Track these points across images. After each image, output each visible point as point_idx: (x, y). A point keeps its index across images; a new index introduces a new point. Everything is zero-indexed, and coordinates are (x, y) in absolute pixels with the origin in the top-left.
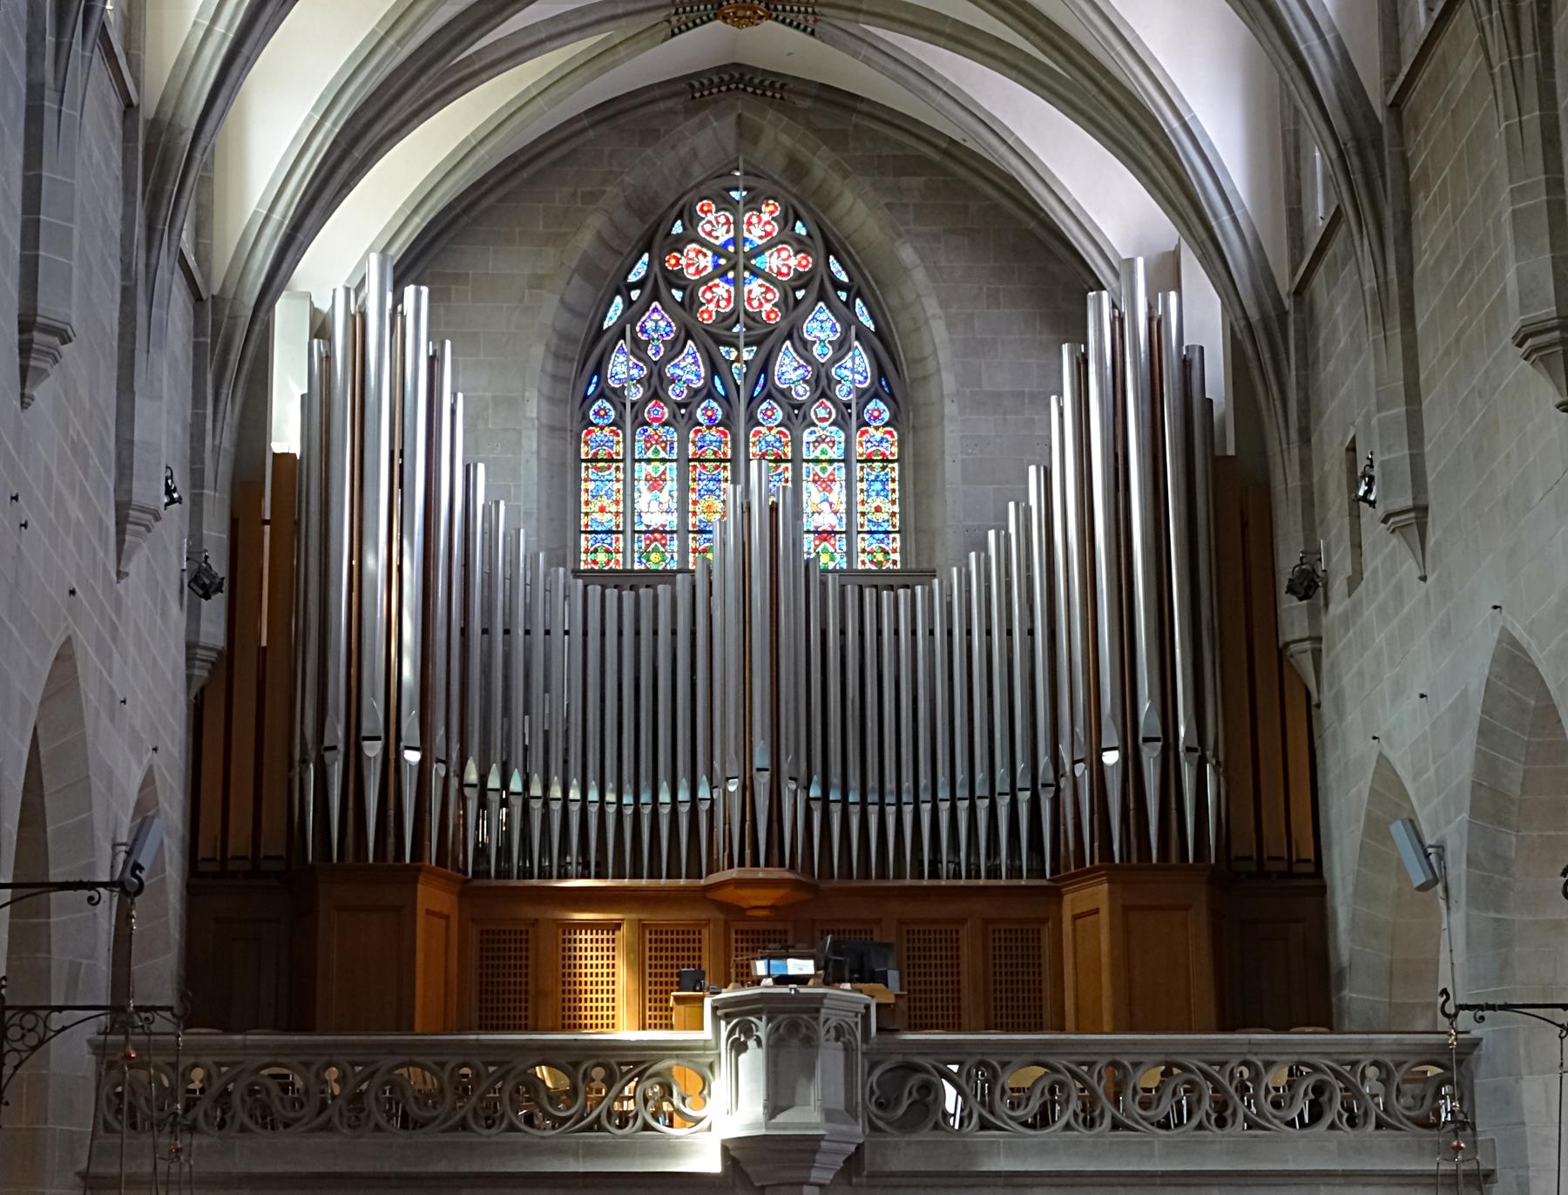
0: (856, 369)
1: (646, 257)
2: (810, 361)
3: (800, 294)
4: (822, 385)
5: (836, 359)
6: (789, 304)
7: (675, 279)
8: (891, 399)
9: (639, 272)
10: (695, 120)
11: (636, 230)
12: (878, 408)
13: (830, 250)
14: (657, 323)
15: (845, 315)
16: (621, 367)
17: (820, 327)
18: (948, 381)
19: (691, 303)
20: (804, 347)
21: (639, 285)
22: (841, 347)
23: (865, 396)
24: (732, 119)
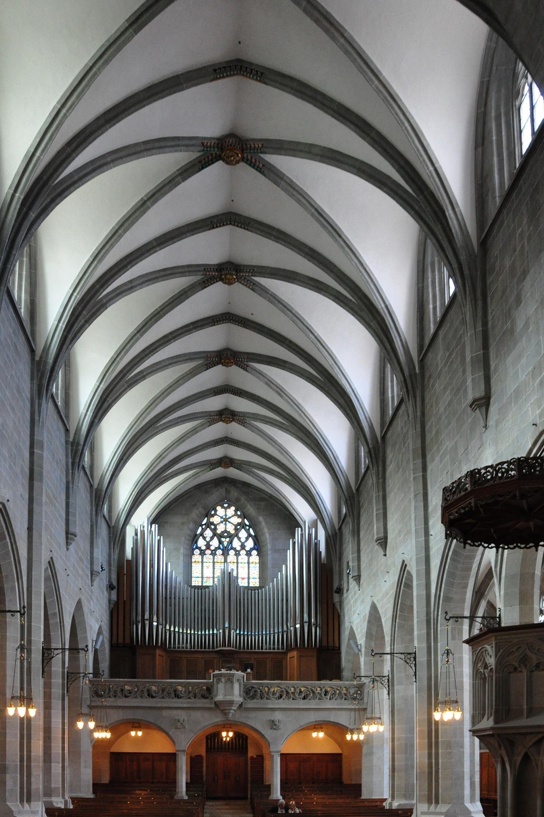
0: (250, 544)
1: (206, 518)
2: (240, 541)
3: (238, 527)
4: (243, 547)
5: (246, 541)
6: (236, 530)
7: (212, 523)
8: (257, 550)
9: (205, 522)
10: (217, 489)
11: (204, 512)
12: (254, 552)
13: (245, 517)
14: (208, 533)
15: (248, 531)
16: (201, 543)
17: (243, 534)
18: (269, 546)
19: (215, 529)
20: (239, 539)
21: (205, 524)
22: (247, 539)
23: (252, 549)
24: (224, 489)
